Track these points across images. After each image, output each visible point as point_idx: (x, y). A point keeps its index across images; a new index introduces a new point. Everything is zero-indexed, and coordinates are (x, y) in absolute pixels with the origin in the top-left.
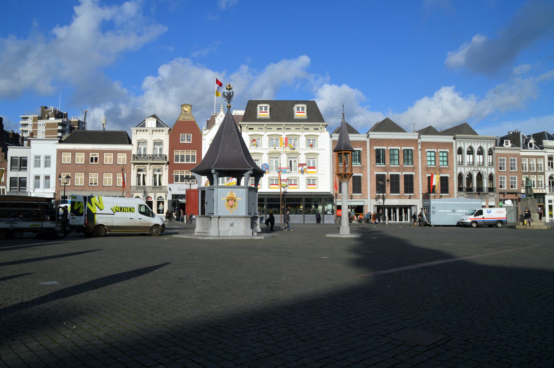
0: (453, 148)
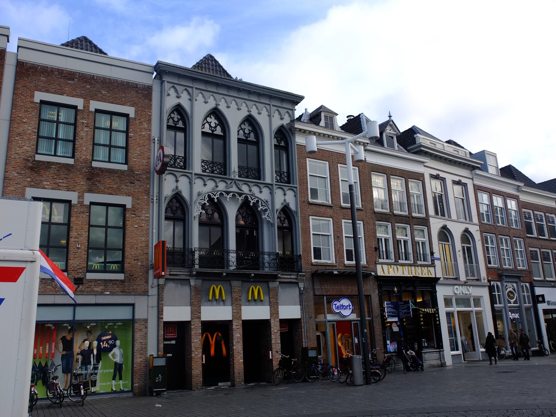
0: (150, 107)
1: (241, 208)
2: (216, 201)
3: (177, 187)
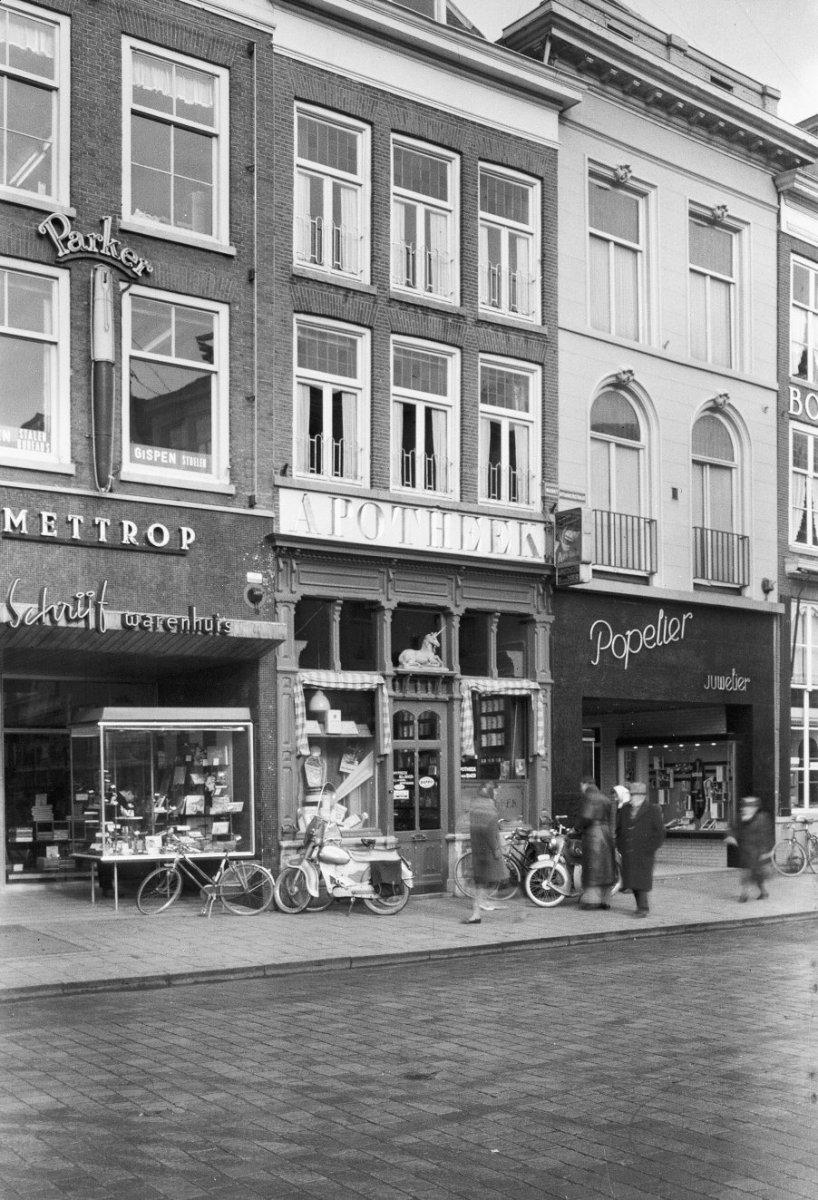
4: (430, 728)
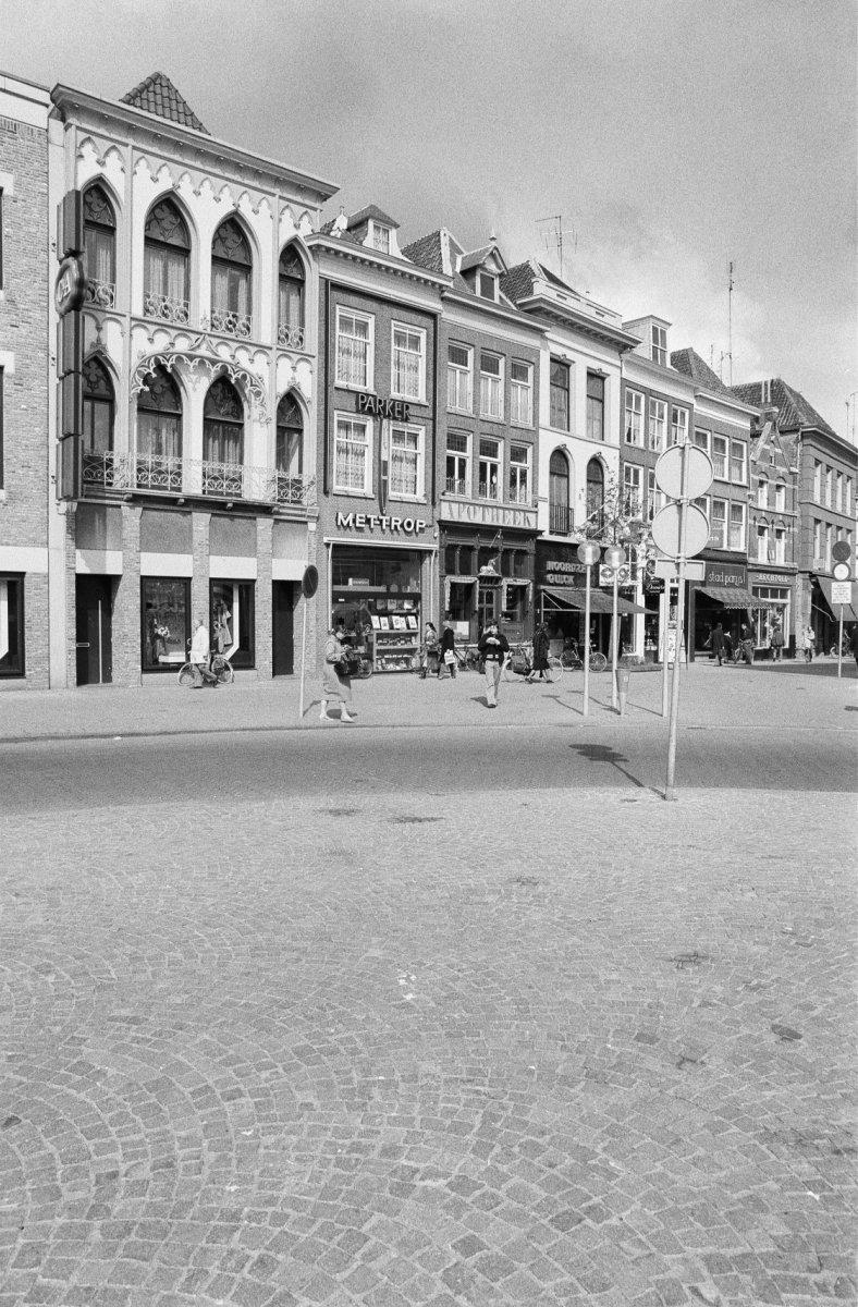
1: (214, 385)
2: (169, 370)
3: (99, 340)
4: (490, 600)
